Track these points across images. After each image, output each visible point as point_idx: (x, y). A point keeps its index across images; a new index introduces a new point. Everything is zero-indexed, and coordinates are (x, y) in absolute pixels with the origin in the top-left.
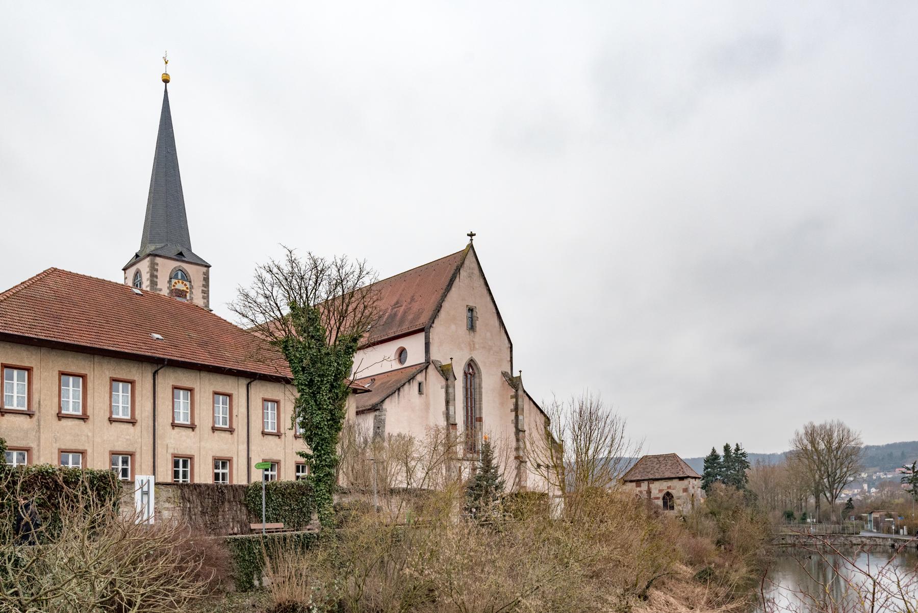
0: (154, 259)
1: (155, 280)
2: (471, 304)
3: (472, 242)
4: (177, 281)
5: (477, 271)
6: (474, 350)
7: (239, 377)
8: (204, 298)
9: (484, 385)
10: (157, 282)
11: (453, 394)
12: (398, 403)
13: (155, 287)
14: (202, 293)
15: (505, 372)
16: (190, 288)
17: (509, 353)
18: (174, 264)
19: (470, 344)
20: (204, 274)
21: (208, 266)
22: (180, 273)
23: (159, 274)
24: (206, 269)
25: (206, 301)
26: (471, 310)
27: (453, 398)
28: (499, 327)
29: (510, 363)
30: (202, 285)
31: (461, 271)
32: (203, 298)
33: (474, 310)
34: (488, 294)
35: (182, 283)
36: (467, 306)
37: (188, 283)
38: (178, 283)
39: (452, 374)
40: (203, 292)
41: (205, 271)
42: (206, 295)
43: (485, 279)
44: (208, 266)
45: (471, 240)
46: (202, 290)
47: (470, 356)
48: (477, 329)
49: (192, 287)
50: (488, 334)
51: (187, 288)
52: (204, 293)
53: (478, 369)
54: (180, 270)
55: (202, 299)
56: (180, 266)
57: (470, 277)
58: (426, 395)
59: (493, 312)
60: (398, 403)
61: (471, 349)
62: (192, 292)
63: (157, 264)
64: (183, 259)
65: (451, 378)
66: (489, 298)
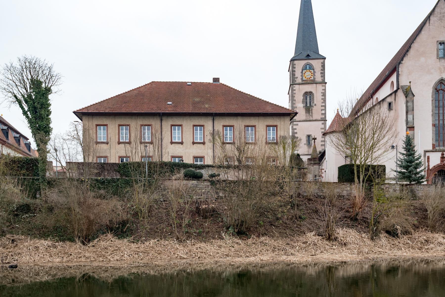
1: (294, 73)
4: (306, 71)
8: (322, 77)
10: (295, 74)
13: (294, 77)
16: (314, 73)
18: (304, 62)
20: (322, 63)
21: (325, 58)
22: (308, 66)
23: (296, 70)
24: (323, 60)
25: (323, 78)
35: (309, 71)
36: (437, 41)
37: (312, 71)
40: (321, 73)
41: (322, 61)
42: (323, 75)
44: (325, 58)
46: (321, 72)
47: (440, 77)
49: (314, 72)
51: (312, 73)
52: (322, 74)
55: (321, 78)
56: (308, 62)
62: (315, 75)
63: (295, 64)
64: (311, 58)
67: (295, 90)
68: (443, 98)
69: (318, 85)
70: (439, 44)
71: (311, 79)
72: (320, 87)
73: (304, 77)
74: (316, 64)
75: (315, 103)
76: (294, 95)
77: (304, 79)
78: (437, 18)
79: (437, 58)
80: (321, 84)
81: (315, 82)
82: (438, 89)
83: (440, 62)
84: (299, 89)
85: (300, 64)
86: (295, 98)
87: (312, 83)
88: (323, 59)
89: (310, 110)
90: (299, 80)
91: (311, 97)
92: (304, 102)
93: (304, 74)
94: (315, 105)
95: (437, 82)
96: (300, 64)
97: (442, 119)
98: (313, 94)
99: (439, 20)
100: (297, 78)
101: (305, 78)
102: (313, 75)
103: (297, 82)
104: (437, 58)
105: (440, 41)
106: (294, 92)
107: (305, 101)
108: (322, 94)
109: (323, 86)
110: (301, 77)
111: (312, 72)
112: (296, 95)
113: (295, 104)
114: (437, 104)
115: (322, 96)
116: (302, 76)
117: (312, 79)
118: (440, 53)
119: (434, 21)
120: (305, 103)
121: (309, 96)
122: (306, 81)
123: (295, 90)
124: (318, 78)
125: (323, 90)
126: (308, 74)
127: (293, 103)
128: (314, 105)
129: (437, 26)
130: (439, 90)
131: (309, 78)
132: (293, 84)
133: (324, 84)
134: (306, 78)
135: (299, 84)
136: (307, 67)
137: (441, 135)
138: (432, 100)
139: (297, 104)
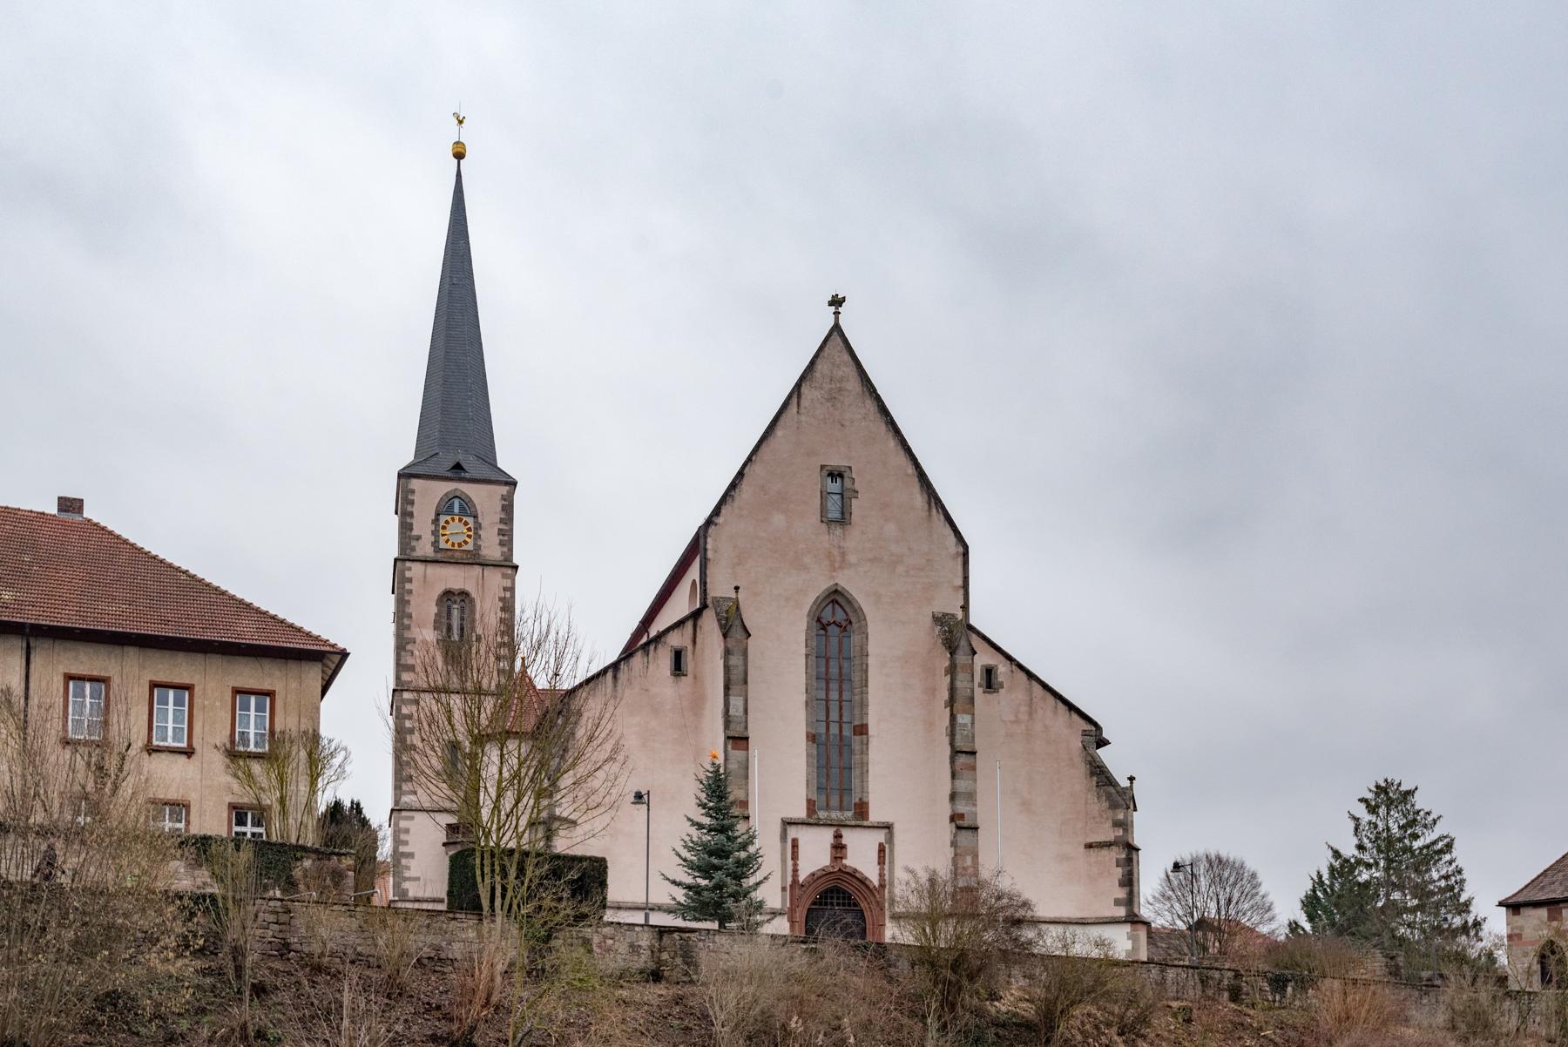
0: (407, 483)
1: (408, 520)
2: (835, 462)
3: (837, 319)
4: (449, 518)
5: (853, 385)
7: (208, 655)
8: (502, 544)
9: (872, 648)
10: (412, 524)
13: (408, 533)
14: (499, 534)
15: (945, 615)
16: (476, 529)
17: (960, 568)
18: (443, 488)
19: (829, 555)
20: (503, 498)
21: (514, 484)
22: (456, 502)
23: (415, 509)
24: (507, 488)
25: (505, 549)
26: (836, 475)
27: (741, 676)
28: (926, 507)
29: (961, 592)
30: (498, 521)
31: (803, 390)
32: (500, 544)
33: (846, 475)
34: (891, 434)
35: (460, 520)
36: (822, 467)
37: (470, 520)
38: (451, 522)
39: (737, 623)
40: (501, 533)
41: (505, 493)
42: (506, 538)
43: (878, 399)
44: (514, 484)
45: (837, 313)
46: (499, 529)
47: (832, 583)
48: (854, 518)
49: (478, 526)
50: (891, 528)
51: (469, 529)
52: (503, 535)
53: (855, 611)
54: (457, 497)
55: (499, 547)
56: (456, 490)
57: (831, 399)
58: (695, 678)
59: (908, 475)
61: (832, 565)
63: (413, 492)
65: (737, 633)
66: (892, 443)
67: (410, 580)
68: (840, 651)
69: (488, 571)
70: (829, 475)
71: (465, 547)
72: (495, 578)
73: (442, 539)
74: (484, 497)
75: (479, 631)
76: (406, 598)
77: (442, 545)
78: (822, 392)
81: (478, 561)
82: (824, 621)
84: (425, 577)
85: (430, 493)
86: (411, 609)
87: (470, 561)
88: (507, 483)
90: (425, 548)
93: (444, 528)
96: (430, 493)
97: (837, 719)
98: (472, 601)
99: (828, 400)
100: (418, 538)
101: (447, 541)
102: (471, 533)
103: (418, 553)
104: (822, 521)
105: (829, 468)
106: (408, 586)
107: (442, 623)
109: (504, 576)
110: (433, 539)
111: (471, 525)
112: (413, 600)
113: (409, 627)
114: (823, 669)
117: (470, 547)
118: (829, 504)
119: (812, 400)
120: (444, 630)
122: (450, 553)
123: (410, 580)
124: (492, 551)
126: (456, 531)
127: (403, 623)
129: (822, 417)
130: (829, 624)
131: (460, 545)
132: (406, 557)
133: (509, 571)
134: (450, 542)
135: (425, 561)
138: (807, 656)
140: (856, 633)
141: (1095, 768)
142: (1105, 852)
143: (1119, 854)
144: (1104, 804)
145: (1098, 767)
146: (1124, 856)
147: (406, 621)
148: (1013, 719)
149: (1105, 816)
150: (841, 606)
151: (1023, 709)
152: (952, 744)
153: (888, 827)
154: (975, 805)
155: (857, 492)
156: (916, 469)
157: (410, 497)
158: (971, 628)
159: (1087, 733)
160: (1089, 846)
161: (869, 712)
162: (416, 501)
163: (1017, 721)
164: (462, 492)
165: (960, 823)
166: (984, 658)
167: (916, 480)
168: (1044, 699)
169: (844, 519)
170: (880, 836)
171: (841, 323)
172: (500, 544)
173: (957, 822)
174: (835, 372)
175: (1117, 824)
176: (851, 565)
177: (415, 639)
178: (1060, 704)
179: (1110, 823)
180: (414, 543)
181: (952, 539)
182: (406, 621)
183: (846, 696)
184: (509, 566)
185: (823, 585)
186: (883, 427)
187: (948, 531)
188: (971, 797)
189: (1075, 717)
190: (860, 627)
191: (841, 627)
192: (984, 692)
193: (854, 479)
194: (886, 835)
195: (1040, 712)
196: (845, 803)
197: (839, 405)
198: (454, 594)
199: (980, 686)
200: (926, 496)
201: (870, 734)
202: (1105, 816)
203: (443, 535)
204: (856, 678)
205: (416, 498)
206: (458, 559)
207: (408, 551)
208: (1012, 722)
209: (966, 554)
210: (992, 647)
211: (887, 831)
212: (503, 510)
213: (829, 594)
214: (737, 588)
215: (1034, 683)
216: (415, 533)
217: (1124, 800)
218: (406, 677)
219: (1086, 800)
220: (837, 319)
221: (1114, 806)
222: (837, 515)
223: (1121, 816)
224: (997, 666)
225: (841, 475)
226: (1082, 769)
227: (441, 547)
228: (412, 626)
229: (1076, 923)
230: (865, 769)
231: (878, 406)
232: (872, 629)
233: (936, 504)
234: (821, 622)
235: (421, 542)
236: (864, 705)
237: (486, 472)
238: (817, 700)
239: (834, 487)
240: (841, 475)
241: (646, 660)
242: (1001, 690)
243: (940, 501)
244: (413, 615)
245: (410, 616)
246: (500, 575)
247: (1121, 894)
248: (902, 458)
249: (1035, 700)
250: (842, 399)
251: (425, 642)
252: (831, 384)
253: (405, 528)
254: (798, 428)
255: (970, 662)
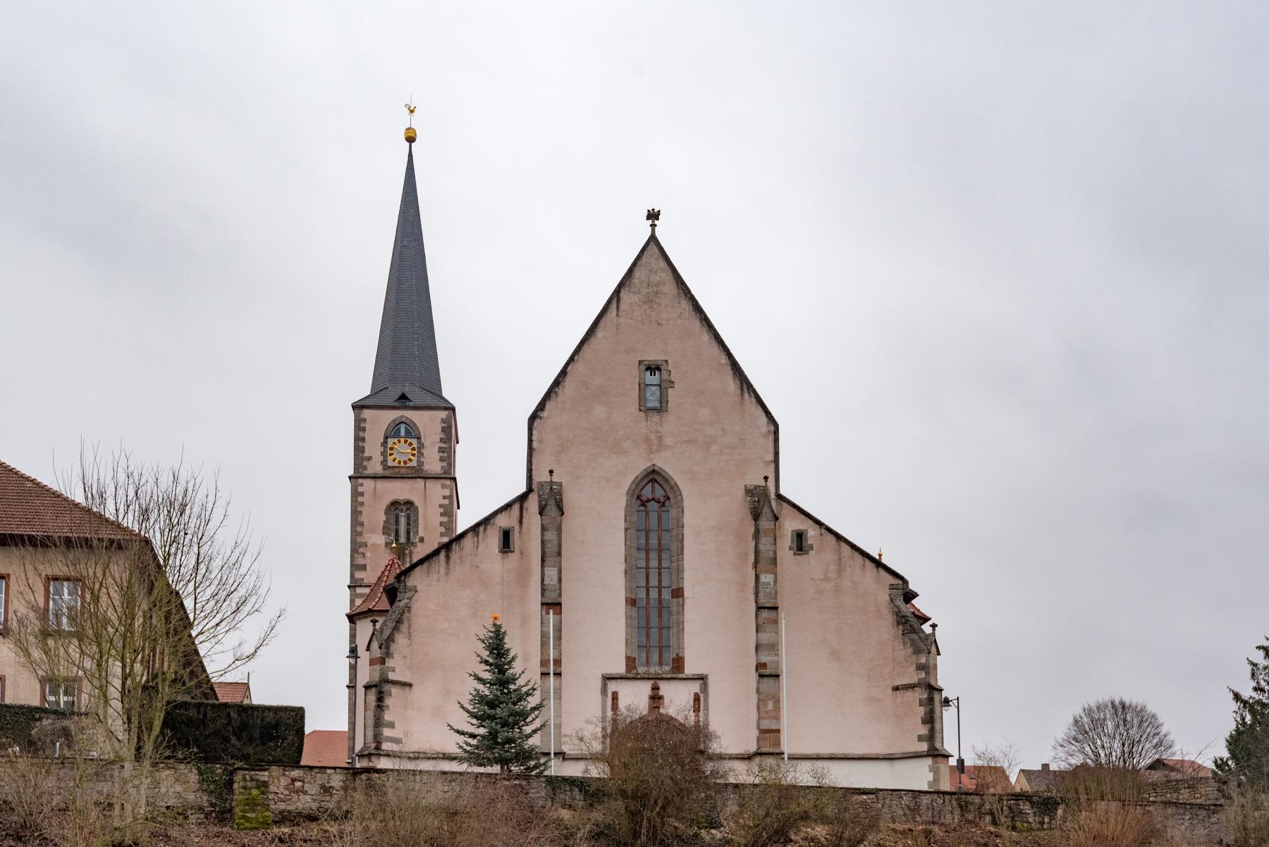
0: (360, 413)
1: (361, 444)
2: (652, 356)
3: (653, 231)
4: (396, 440)
5: (670, 288)
6: (658, 450)
8: (442, 460)
9: (687, 520)
10: (364, 447)
11: (556, 543)
12: (447, 574)
14: (439, 452)
16: (419, 448)
17: (771, 444)
18: (391, 415)
19: (647, 440)
20: (443, 421)
22: (403, 428)
23: (367, 435)
24: (446, 412)
25: (445, 464)
26: (653, 368)
28: (739, 392)
29: (773, 465)
30: (439, 440)
32: (440, 460)
33: (662, 368)
34: (705, 329)
35: (406, 442)
36: (640, 362)
37: (414, 442)
40: (441, 450)
42: (445, 455)
43: (692, 299)
45: (653, 226)
46: (440, 448)
48: (671, 405)
49: (421, 446)
50: (705, 413)
53: (672, 488)
54: (403, 422)
56: (402, 416)
59: (722, 365)
60: (447, 574)
62: (423, 454)
63: (365, 420)
66: (706, 337)
67: (362, 494)
68: (659, 523)
69: (430, 483)
70: (647, 369)
71: (410, 464)
72: (437, 491)
73: (390, 458)
74: (429, 424)
75: (421, 534)
76: (359, 509)
77: (390, 463)
78: (640, 296)
79: (640, 410)
80: (438, 481)
81: (420, 475)
82: (644, 498)
83: (647, 420)
84: (375, 491)
85: (381, 420)
86: (362, 519)
87: (414, 475)
88: (446, 409)
89: (404, 553)
90: (375, 467)
91: (412, 518)
92: (389, 529)
93: (392, 449)
94: (422, 540)
95: (639, 478)
96: (381, 420)
97: (657, 584)
98: (416, 509)
99: (645, 303)
100: (369, 459)
101: (394, 460)
102: (415, 452)
103: (370, 471)
104: (640, 410)
105: (647, 363)
106: (360, 499)
107: (390, 528)
108: (442, 510)
109: (443, 487)
110: (382, 459)
111: (415, 445)
112: (365, 510)
113: (361, 534)
114: (644, 541)
115: (442, 515)
116: (384, 454)
117: (414, 464)
118: (648, 394)
119: (630, 303)
120: (393, 534)
121: (403, 514)
122: (397, 470)
123: (362, 494)
124: (433, 464)
125: (444, 497)
126: (402, 451)
127: (356, 531)
128: (417, 540)
129: (639, 318)
130: (649, 501)
132: (359, 475)
134: (397, 461)
135: (375, 477)
136: (400, 428)
137: (654, 631)
138: (626, 530)
139: (368, 535)
140: (674, 507)
141: (901, 617)
142: (909, 693)
143: (921, 694)
144: (909, 650)
145: (904, 616)
146: (926, 696)
147: (359, 529)
148: (822, 577)
149: (910, 661)
150: (660, 485)
151: (833, 568)
152: (756, 602)
153: (702, 678)
154: (777, 655)
155: (673, 382)
156: (729, 358)
157: (362, 425)
158: (780, 497)
159: (895, 587)
160: (896, 689)
161: (685, 577)
162: (367, 428)
163: (826, 579)
164: (407, 418)
165: (762, 671)
166: (791, 524)
167: (730, 368)
168: (852, 558)
169: (661, 409)
170: (695, 687)
171: (658, 234)
172: (440, 460)
173: (760, 671)
174: (652, 278)
175: (920, 667)
176: (668, 447)
177: (366, 543)
178: (868, 562)
179: (913, 668)
180: (365, 463)
181: (763, 419)
182: (359, 529)
183: (665, 564)
184: (448, 478)
185: (640, 466)
186: (698, 323)
187: (760, 412)
188: (774, 647)
189: (882, 572)
190: (676, 502)
191: (660, 502)
192: (794, 555)
193: (670, 371)
194: (701, 684)
195: (848, 569)
196: (665, 660)
197: (656, 307)
198: (400, 503)
199: (791, 548)
200: (738, 382)
201: (685, 596)
202: (910, 661)
203: (391, 455)
204: (674, 547)
205: (367, 425)
206: (403, 474)
207: (360, 470)
208: (822, 580)
209: (776, 432)
210: (802, 513)
211: (701, 682)
212: (442, 431)
213: (648, 474)
214: (551, 472)
215: (842, 544)
216: (366, 454)
217: (926, 645)
218: (359, 575)
219: (894, 647)
220: (653, 231)
221: (917, 651)
222: (657, 404)
223: (923, 660)
224: (807, 530)
225: (658, 368)
226: (889, 619)
227: (388, 465)
228: (364, 532)
229: (884, 759)
230: (681, 627)
231: (693, 305)
232: (687, 504)
233: (748, 389)
234: (641, 500)
235: (372, 462)
236: (680, 571)
237: (430, 400)
238: (637, 568)
239: (651, 379)
240: (658, 368)
241: (476, 540)
242: (810, 552)
243: (752, 386)
244: (365, 524)
245: (362, 524)
246: (440, 486)
247: (924, 730)
248: (716, 350)
249: (843, 559)
250: (658, 300)
251: (375, 545)
252: (648, 289)
253: (359, 450)
254: (618, 329)
255: (773, 527)
